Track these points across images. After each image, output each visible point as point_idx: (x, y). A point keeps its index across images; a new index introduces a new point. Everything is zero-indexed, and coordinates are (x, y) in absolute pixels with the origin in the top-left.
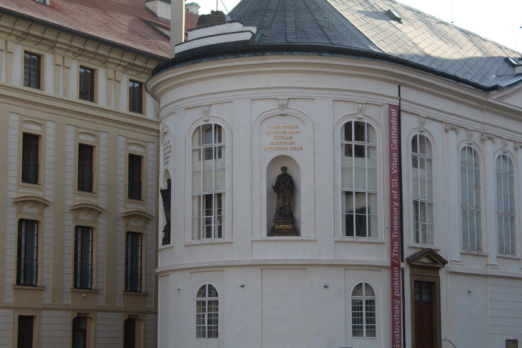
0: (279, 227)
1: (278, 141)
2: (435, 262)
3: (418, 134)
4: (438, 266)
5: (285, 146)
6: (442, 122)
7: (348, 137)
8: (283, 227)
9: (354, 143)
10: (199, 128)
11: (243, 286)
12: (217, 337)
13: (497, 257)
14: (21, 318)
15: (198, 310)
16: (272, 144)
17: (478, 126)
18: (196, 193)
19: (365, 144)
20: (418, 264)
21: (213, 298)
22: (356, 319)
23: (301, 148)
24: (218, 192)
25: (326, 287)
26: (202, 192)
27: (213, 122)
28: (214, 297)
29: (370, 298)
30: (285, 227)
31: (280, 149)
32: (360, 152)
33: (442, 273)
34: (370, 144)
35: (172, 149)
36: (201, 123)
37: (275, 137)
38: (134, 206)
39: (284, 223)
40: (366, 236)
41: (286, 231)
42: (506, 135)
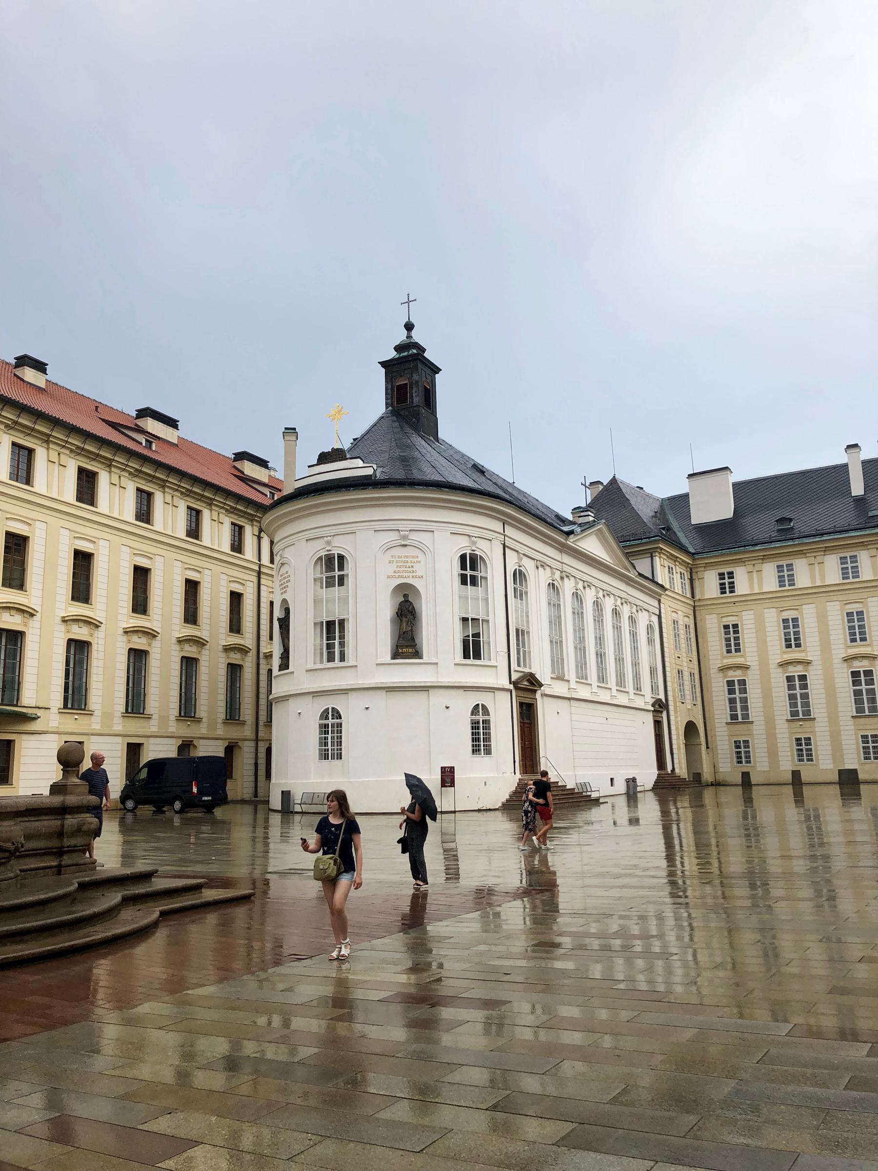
1: (400, 569)
2: (532, 684)
3: (517, 568)
4: (536, 688)
5: (407, 574)
6: (534, 559)
7: (463, 567)
9: (469, 572)
10: (320, 558)
11: (367, 708)
12: (341, 758)
13: (576, 682)
14: (129, 745)
15: (321, 733)
16: (395, 572)
17: (559, 566)
18: (319, 620)
19: (478, 574)
20: (522, 686)
21: (336, 721)
22: (475, 739)
23: (422, 577)
24: (342, 617)
25: (447, 708)
27: (335, 552)
28: (337, 719)
29: (486, 718)
31: (402, 577)
32: (474, 581)
33: (538, 695)
34: (483, 574)
35: (292, 578)
36: (323, 554)
37: (398, 566)
38: (234, 640)
39: (407, 646)
40: (481, 659)
42: (579, 575)
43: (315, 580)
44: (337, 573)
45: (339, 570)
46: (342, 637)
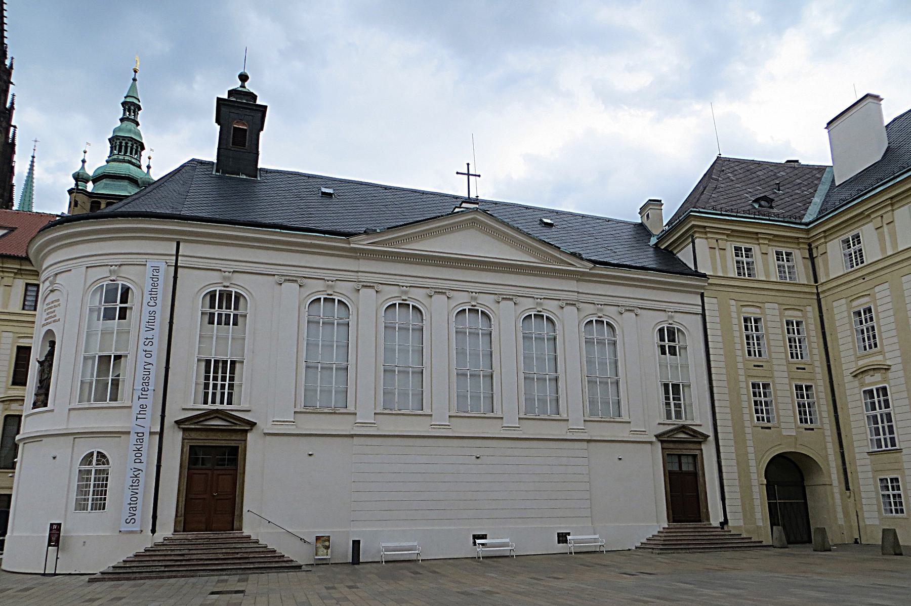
24: (234, 359)
43: (202, 313)
44: (232, 312)
45: (236, 308)
46: (232, 379)
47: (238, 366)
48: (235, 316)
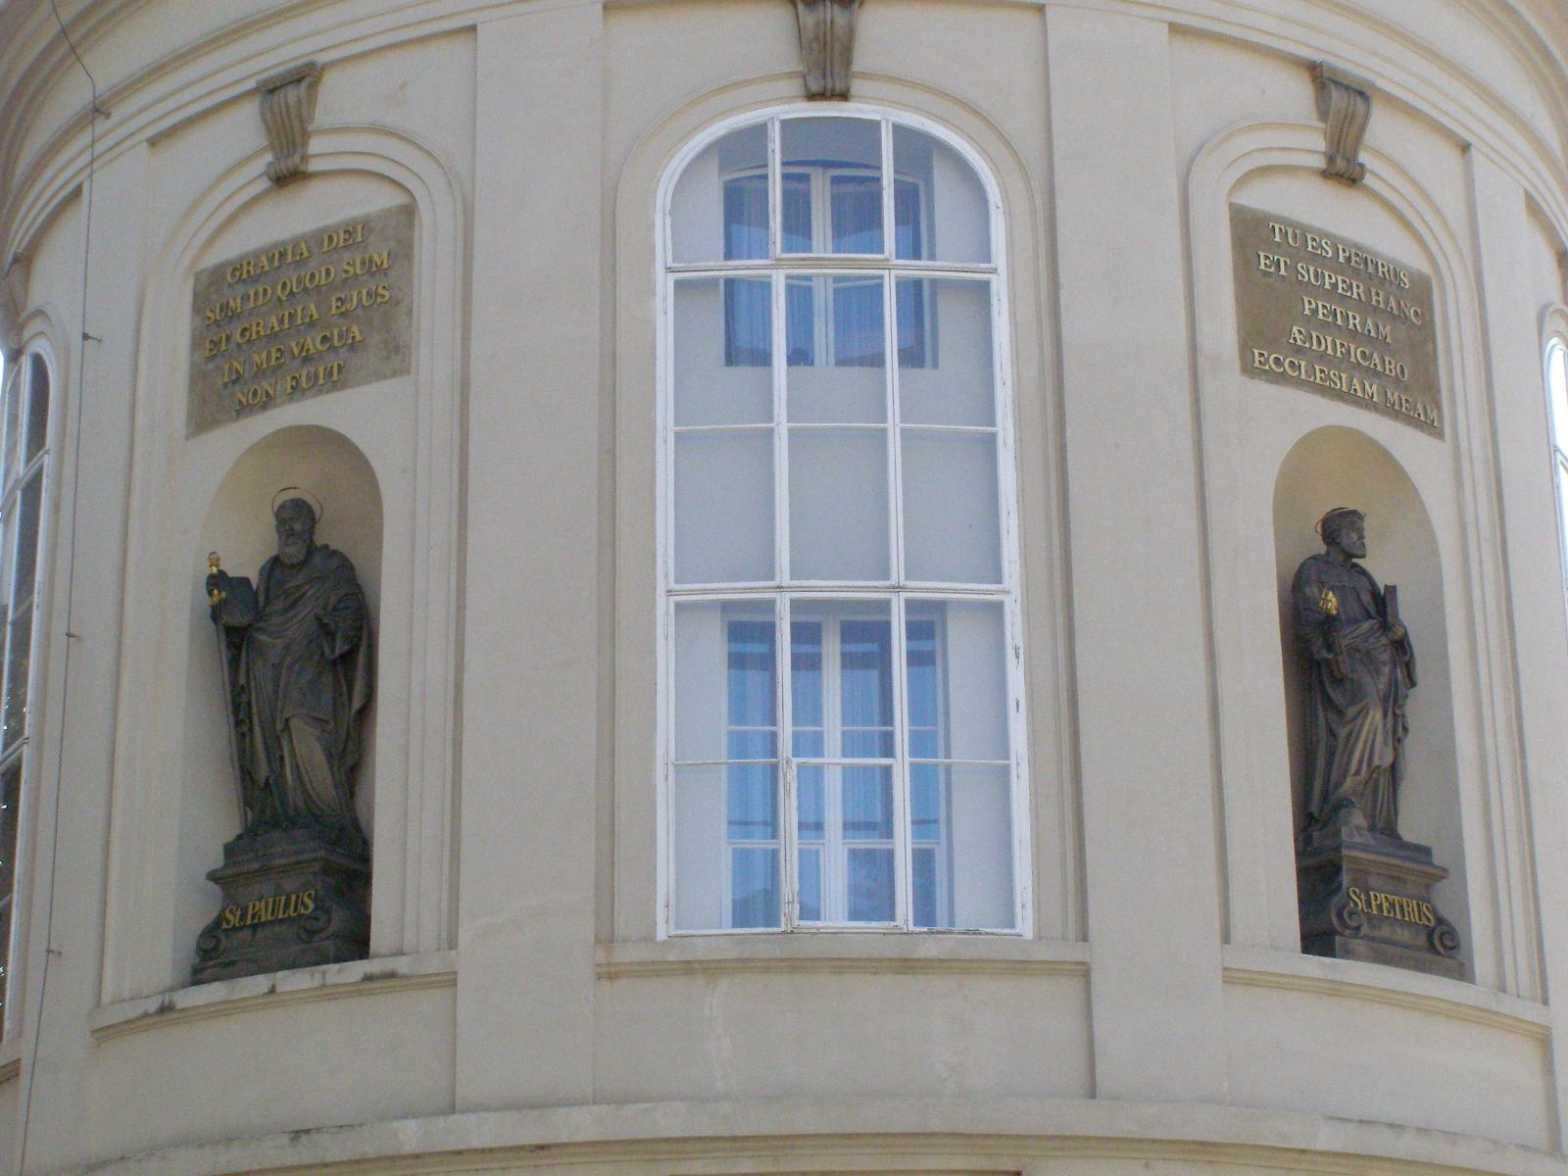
0: (1369, 905)
8: (1393, 905)
24: (930, 589)
26: (786, 581)
30: (1401, 906)
41: (1403, 935)
47: (961, 643)
48: (913, 293)
